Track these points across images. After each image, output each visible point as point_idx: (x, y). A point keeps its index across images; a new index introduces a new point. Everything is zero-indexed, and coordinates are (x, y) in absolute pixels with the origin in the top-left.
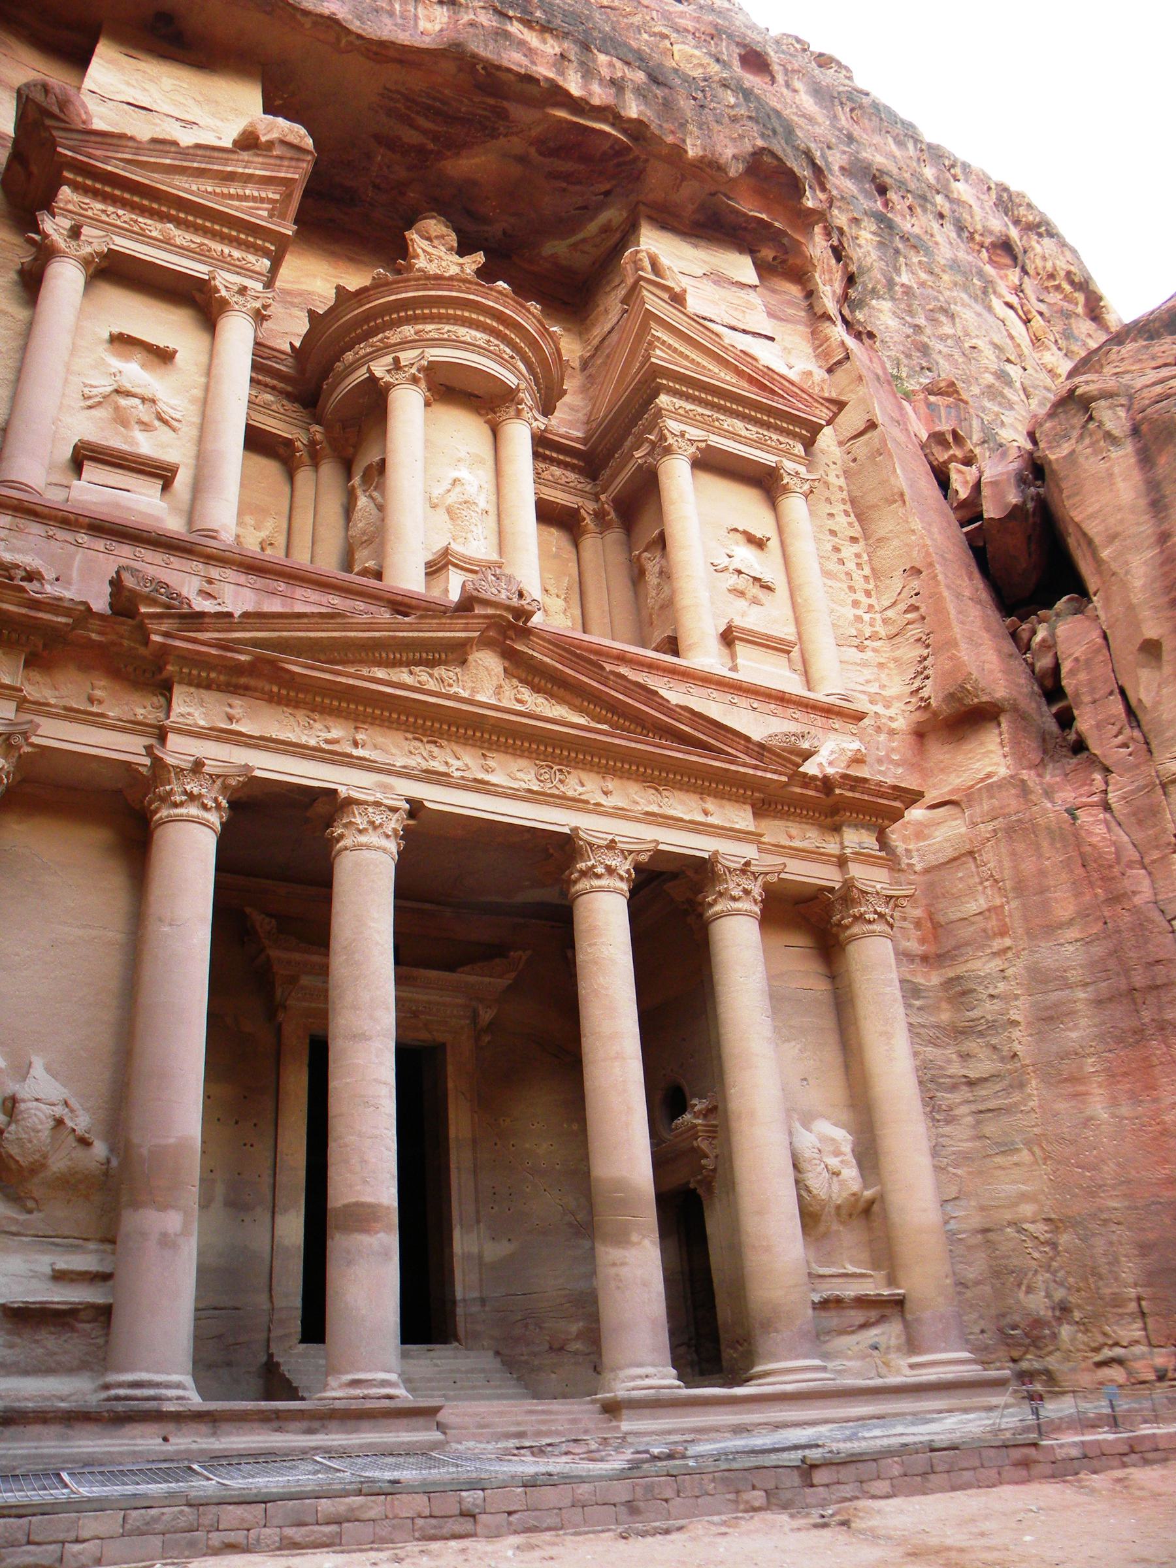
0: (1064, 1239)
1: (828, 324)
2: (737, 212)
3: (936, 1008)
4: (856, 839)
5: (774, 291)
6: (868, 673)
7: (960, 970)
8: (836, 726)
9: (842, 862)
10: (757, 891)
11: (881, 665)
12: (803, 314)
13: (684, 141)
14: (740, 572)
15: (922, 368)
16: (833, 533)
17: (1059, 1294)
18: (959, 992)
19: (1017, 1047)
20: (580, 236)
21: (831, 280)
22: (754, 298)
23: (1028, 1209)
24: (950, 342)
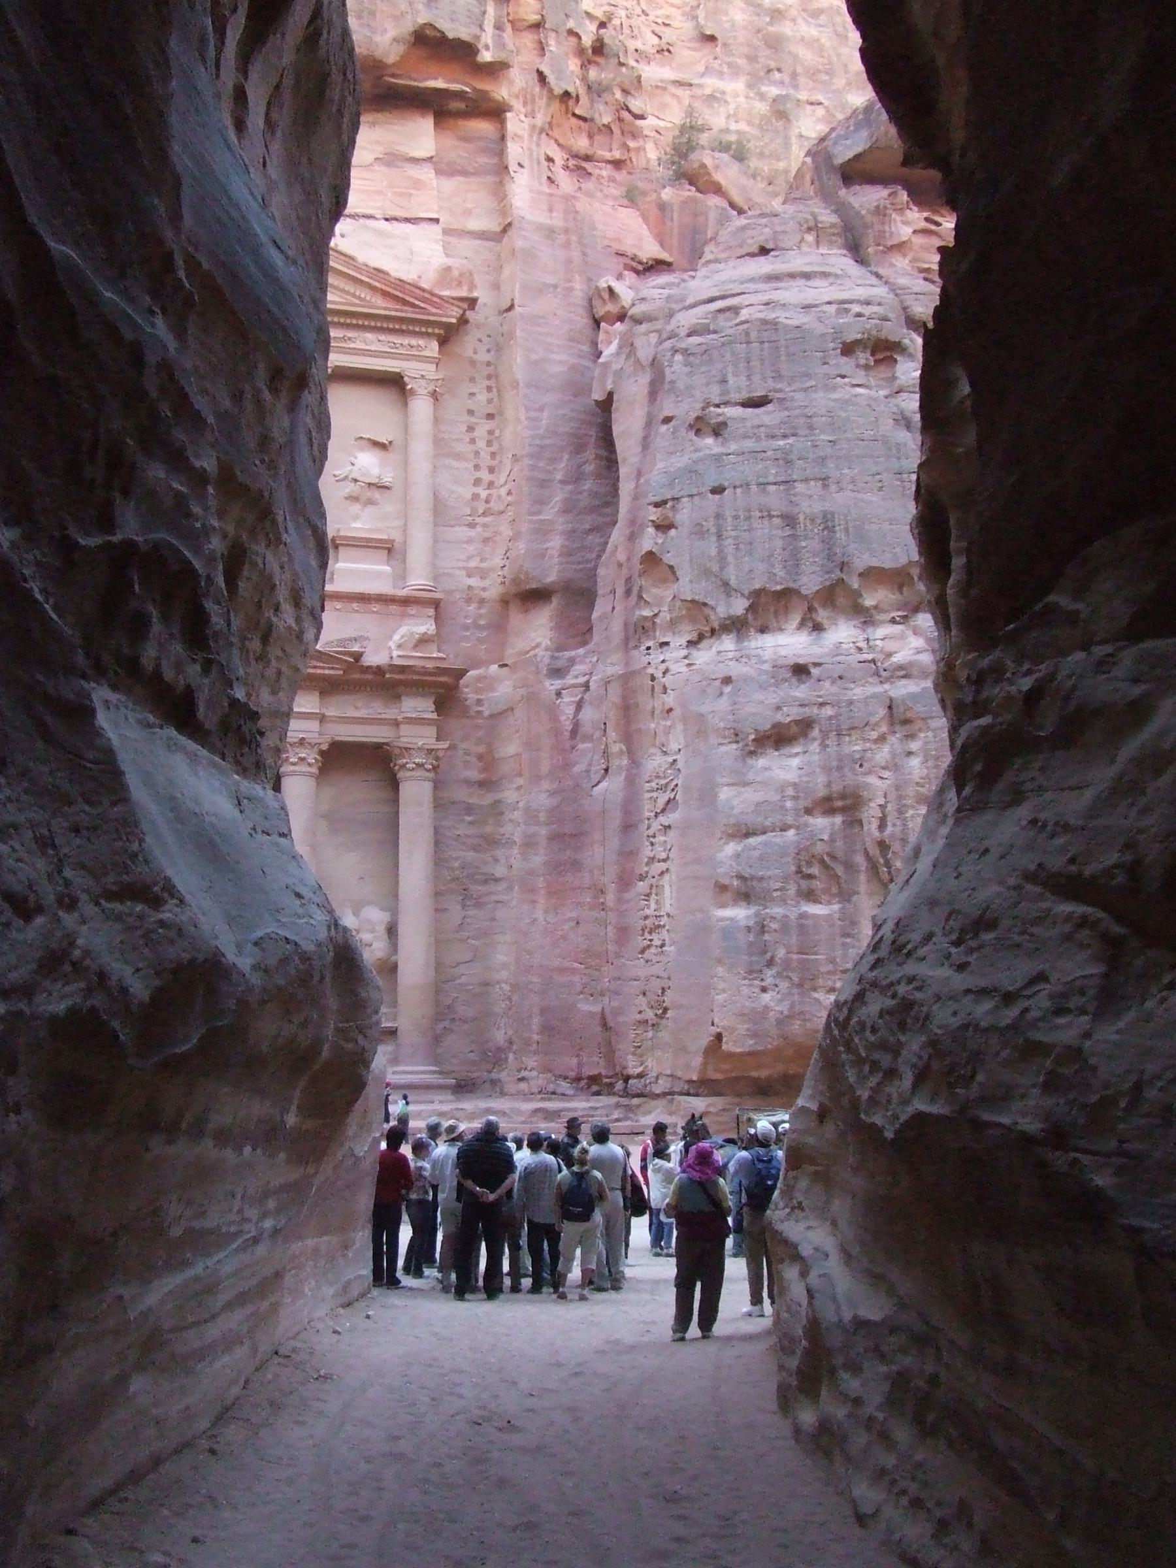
0: (515, 998)
1: (507, 178)
2: (406, 86)
3: (485, 823)
4: (418, 706)
5: (466, 139)
6: (471, 548)
7: (498, 796)
8: (413, 612)
10: (312, 756)
11: (486, 540)
12: (495, 160)
14: (356, 481)
15: (769, 71)
16: (471, 412)
17: (510, 1033)
19: (512, 861)
21: (533, 111)
23: (504, 974)
24: (823, 18)
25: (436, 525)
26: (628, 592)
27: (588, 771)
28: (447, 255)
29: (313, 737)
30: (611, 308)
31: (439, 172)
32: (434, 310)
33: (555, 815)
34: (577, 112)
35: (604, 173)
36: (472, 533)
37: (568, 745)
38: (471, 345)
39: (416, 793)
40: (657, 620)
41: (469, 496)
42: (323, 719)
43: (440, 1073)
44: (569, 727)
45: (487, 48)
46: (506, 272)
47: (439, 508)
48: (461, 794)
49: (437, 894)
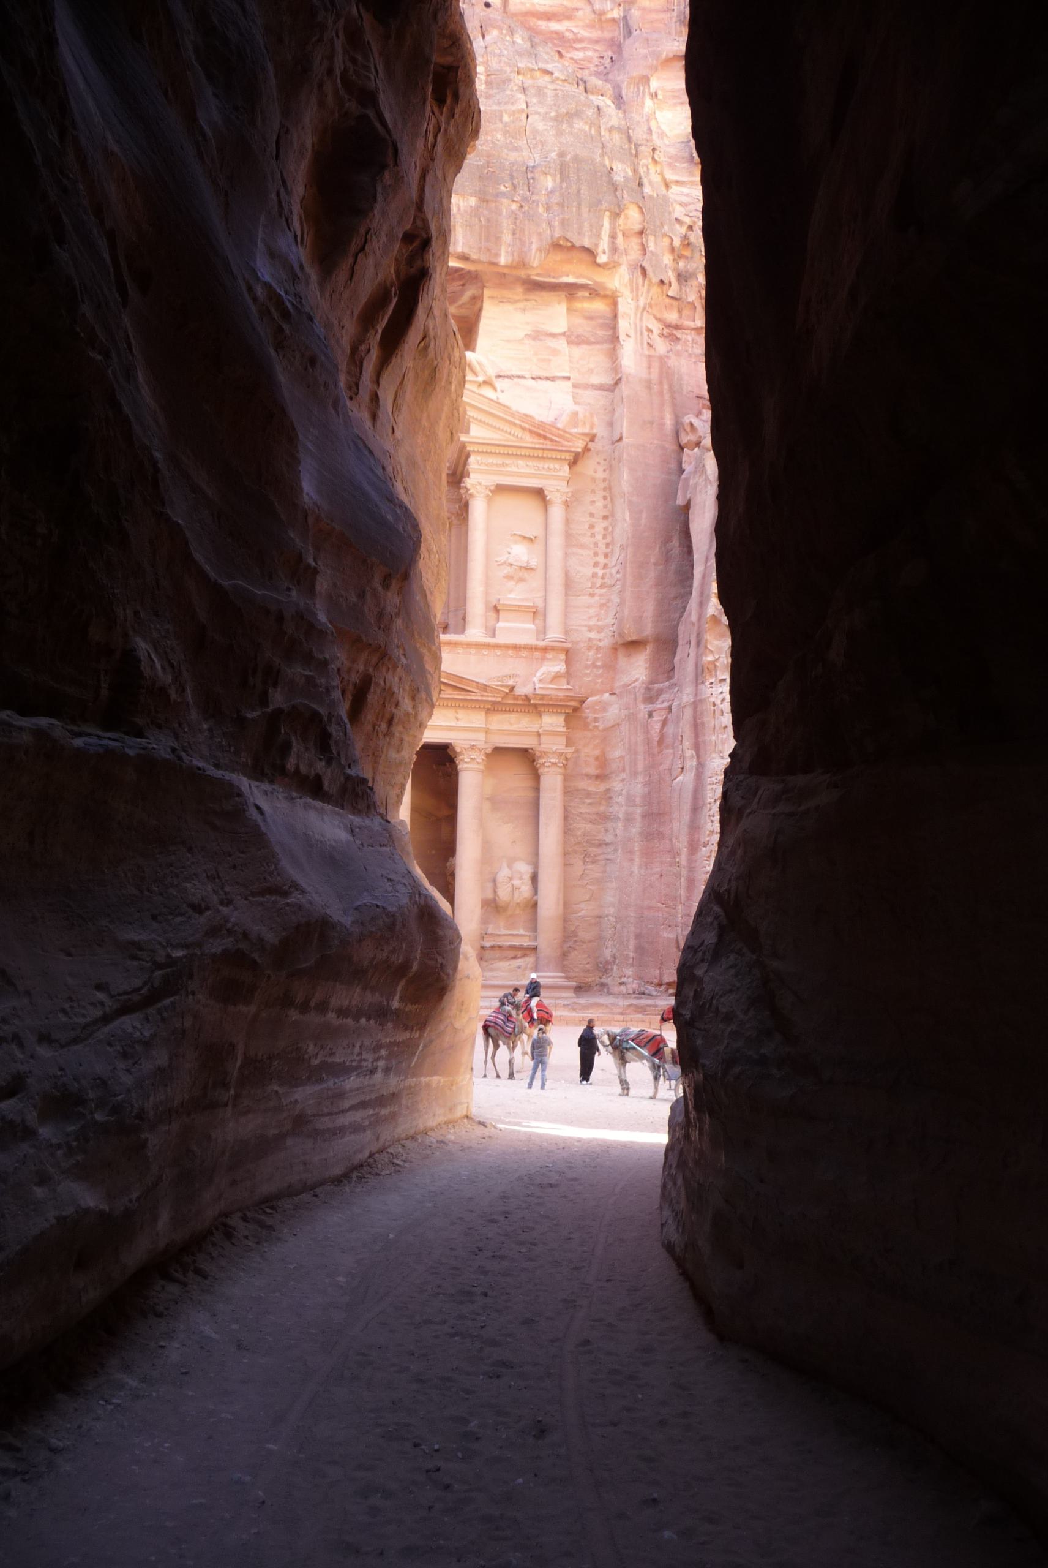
0: (618, 926)
4: (553, 722)
5: (590, 318)
6: (592, 611)
9: (539, 735)
10: (480, 757)
11: (602, 605)
13: (497, 255)
14: (511, 565)
16: (592, 515)
17: (614, 951)
18: (608, 796)
19: (618, 832)
20: (460, 303)
22: (562, 344)
23: (612, 910)
25: (566, 594)
26: (698, 644)
27: (670, 770)
28: (576, 403)
29: (481, 744)
30: (692, 438)
31: (570, 343)
32: (566, 443)
33: (648, 799)
34: (670, 294)
35: (689, 338)
36: (592, 600)
37: (656, 750)
38: (592, 467)
39: (552, 783)
40: (718, 664)
41: (590, 574)
42: (487, 731)
43: (568, 978)
44: (656, 738)
45: (604, 253)
46: (617, 415)
47: (568, 584)
48: (583, 784)
49: (566, 854)
